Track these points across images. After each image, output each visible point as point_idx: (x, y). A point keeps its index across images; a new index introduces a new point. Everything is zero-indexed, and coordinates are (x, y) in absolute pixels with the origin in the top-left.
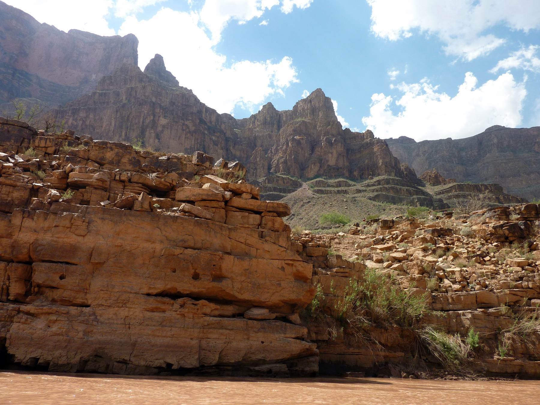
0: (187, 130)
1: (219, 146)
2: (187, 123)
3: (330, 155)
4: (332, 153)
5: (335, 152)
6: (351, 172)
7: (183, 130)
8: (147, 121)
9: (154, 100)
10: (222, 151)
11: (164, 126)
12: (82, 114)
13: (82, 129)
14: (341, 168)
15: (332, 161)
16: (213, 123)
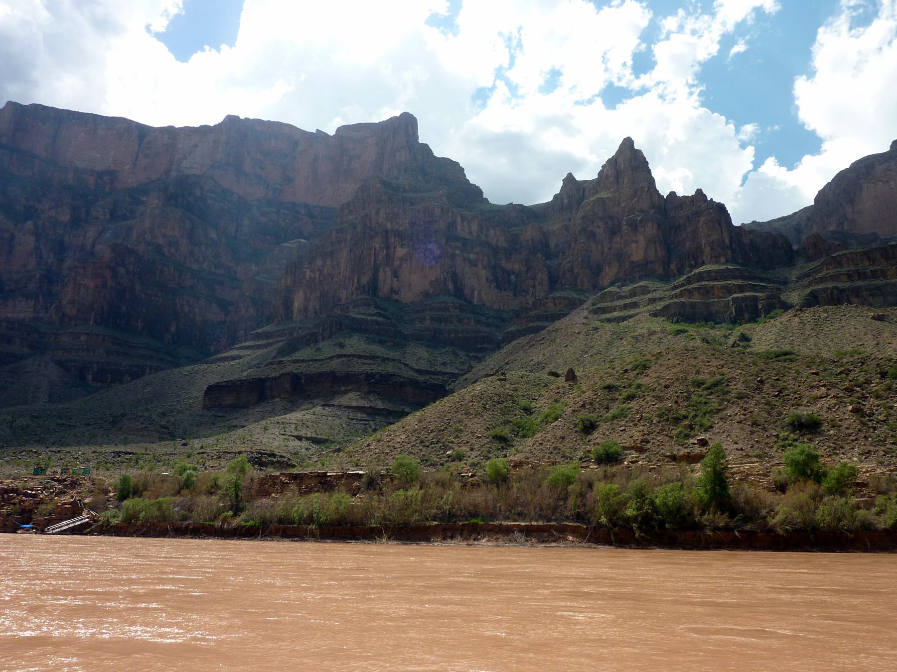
0: (431, 257)
1: (480, 265)
2: (431, 246)
3: (634, 245)
4: (636, 242)
5: (641, 238)
6: (666, 264)
7: (426, 258)
8: (380, 257)
9: (389, 226)
11: (401, 259)
12: (319, 263)
13: (321, 281)
14: (651, 262)
15: (637, 253)
16: (474, 234)
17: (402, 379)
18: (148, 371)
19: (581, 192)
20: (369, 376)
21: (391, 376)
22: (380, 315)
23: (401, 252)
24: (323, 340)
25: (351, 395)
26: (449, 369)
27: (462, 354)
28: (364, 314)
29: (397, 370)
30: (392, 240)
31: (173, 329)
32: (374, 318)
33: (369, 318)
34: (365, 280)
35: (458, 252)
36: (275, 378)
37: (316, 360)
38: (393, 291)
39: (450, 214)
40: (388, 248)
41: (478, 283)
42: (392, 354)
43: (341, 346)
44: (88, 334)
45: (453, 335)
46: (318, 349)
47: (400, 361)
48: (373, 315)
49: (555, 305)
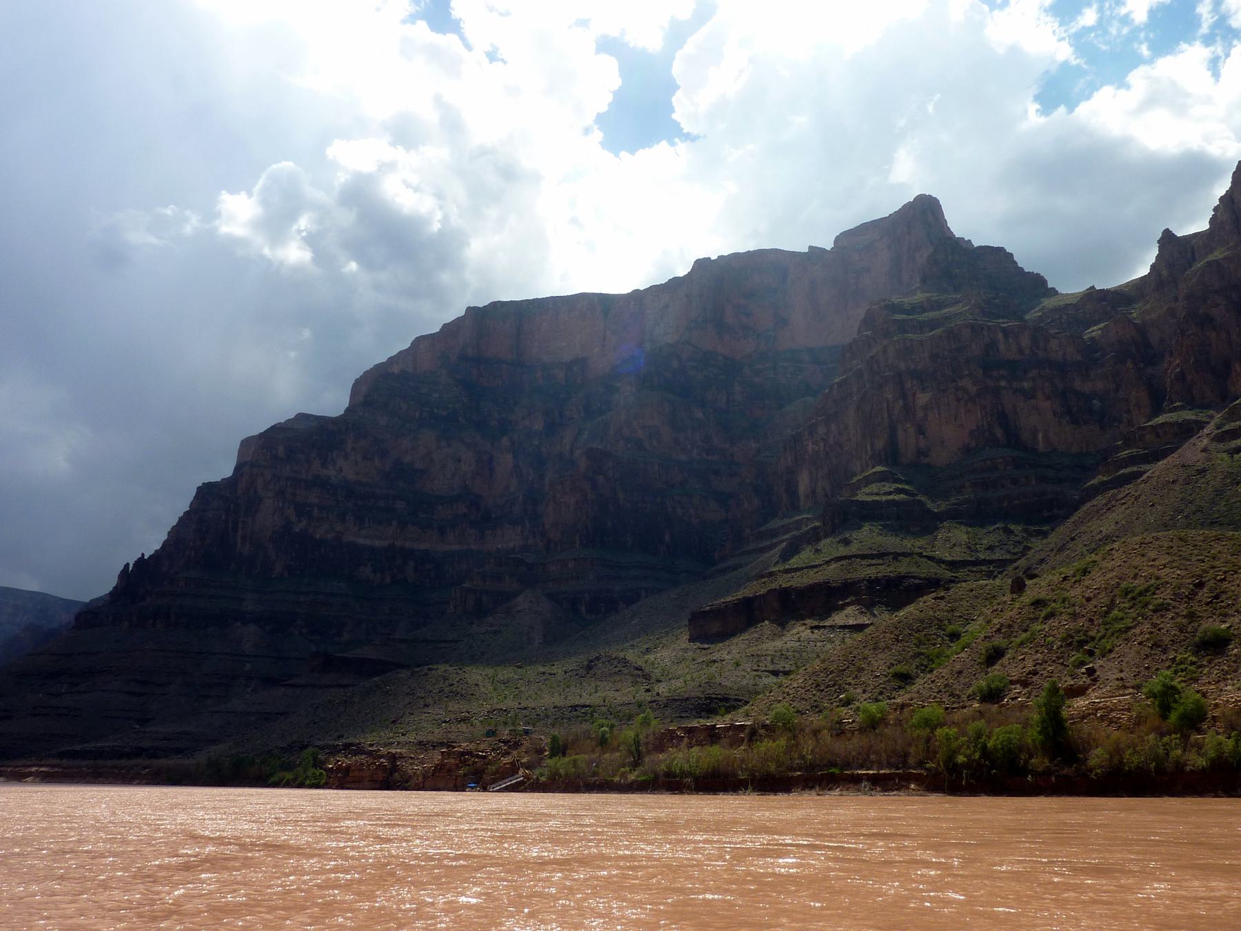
7: (958, 400)
9: (902, 366)
10: (1048, 403)
11: (926, 408)
16: (1027, 352)
17: (917, 581)
18: (643, 594)
19: (1189, 255)
20: (872, 582)
21: (901, 578)
22: (899, 491)
23: (923, 398)
24: (826, 537)
25: (849, 610)
26: (998, 555)
27: (1017, 528)
28: (877, 494)
29: (913, 569)
30: (908, 385)
31: (667, 538)
32: (891, 497)
33: (884, 498)
34: (880, 444)
35: (1003, 383)
36: (762, 596)
37: (812, 567)
38: (921, 453)
39: (985, 333)
40: (904, 396)
41: (1041, 422)
42: (909, 544)
43: (847, 542)
44: (575, 560)
45: (1005, 504)
46: (817, 551)
47: (920, 555)
48: (890, 493)
49: (1158, 436)
